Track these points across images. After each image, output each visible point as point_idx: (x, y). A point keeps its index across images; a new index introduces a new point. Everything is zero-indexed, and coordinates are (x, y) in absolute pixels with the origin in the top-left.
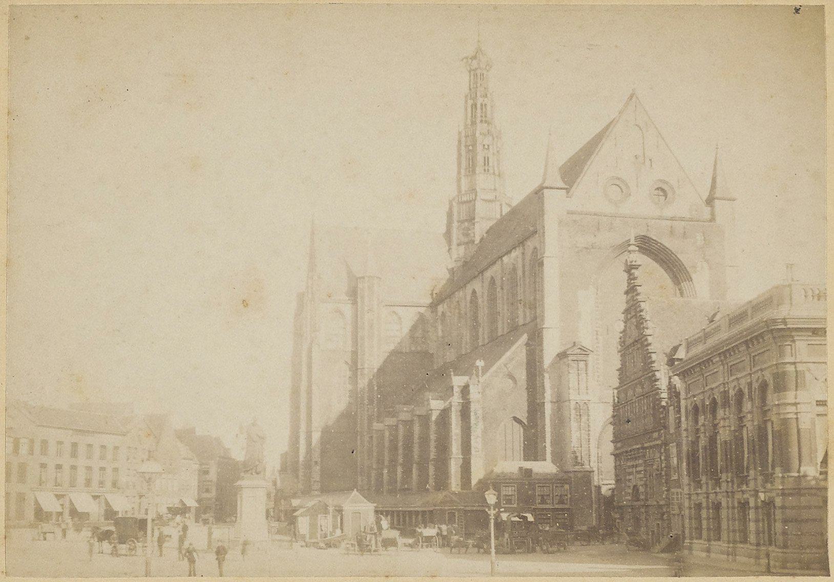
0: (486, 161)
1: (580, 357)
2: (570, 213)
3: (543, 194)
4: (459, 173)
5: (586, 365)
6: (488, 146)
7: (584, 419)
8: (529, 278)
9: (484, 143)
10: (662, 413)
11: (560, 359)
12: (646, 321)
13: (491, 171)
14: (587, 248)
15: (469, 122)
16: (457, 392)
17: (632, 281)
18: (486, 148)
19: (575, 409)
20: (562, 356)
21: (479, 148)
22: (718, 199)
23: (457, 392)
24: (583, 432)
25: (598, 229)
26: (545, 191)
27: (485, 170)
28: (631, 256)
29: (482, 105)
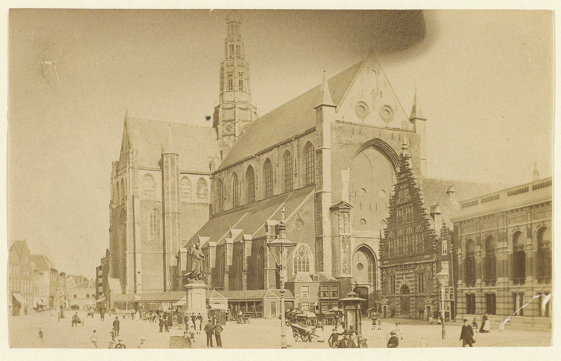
0: (241, 82)
1: (346, 210)
2: (338, 121)
3: (321, 109)
4: (222, 89)
5: (349, 215)
6: (242, 73)
7: (347, 246)
8: (303, 161)
9: (240, 71)
10: (435, 244)
11: (332, 211)
12: (420, 190)
13: (244, 90)
14: (346, 144)
15: (228, 57)
16: (269, 230)
17: (406, 167)
18: (241, 75)
19: (343, 241)
20: (332, 209)
21: (236, 74)
22: (417, 119)
23: (269, 230)
24: (346, 254)
25: (353, 133)
26: (323, 107)
27: (240, 90)
28: (405, 151)
29: (237, 46)
